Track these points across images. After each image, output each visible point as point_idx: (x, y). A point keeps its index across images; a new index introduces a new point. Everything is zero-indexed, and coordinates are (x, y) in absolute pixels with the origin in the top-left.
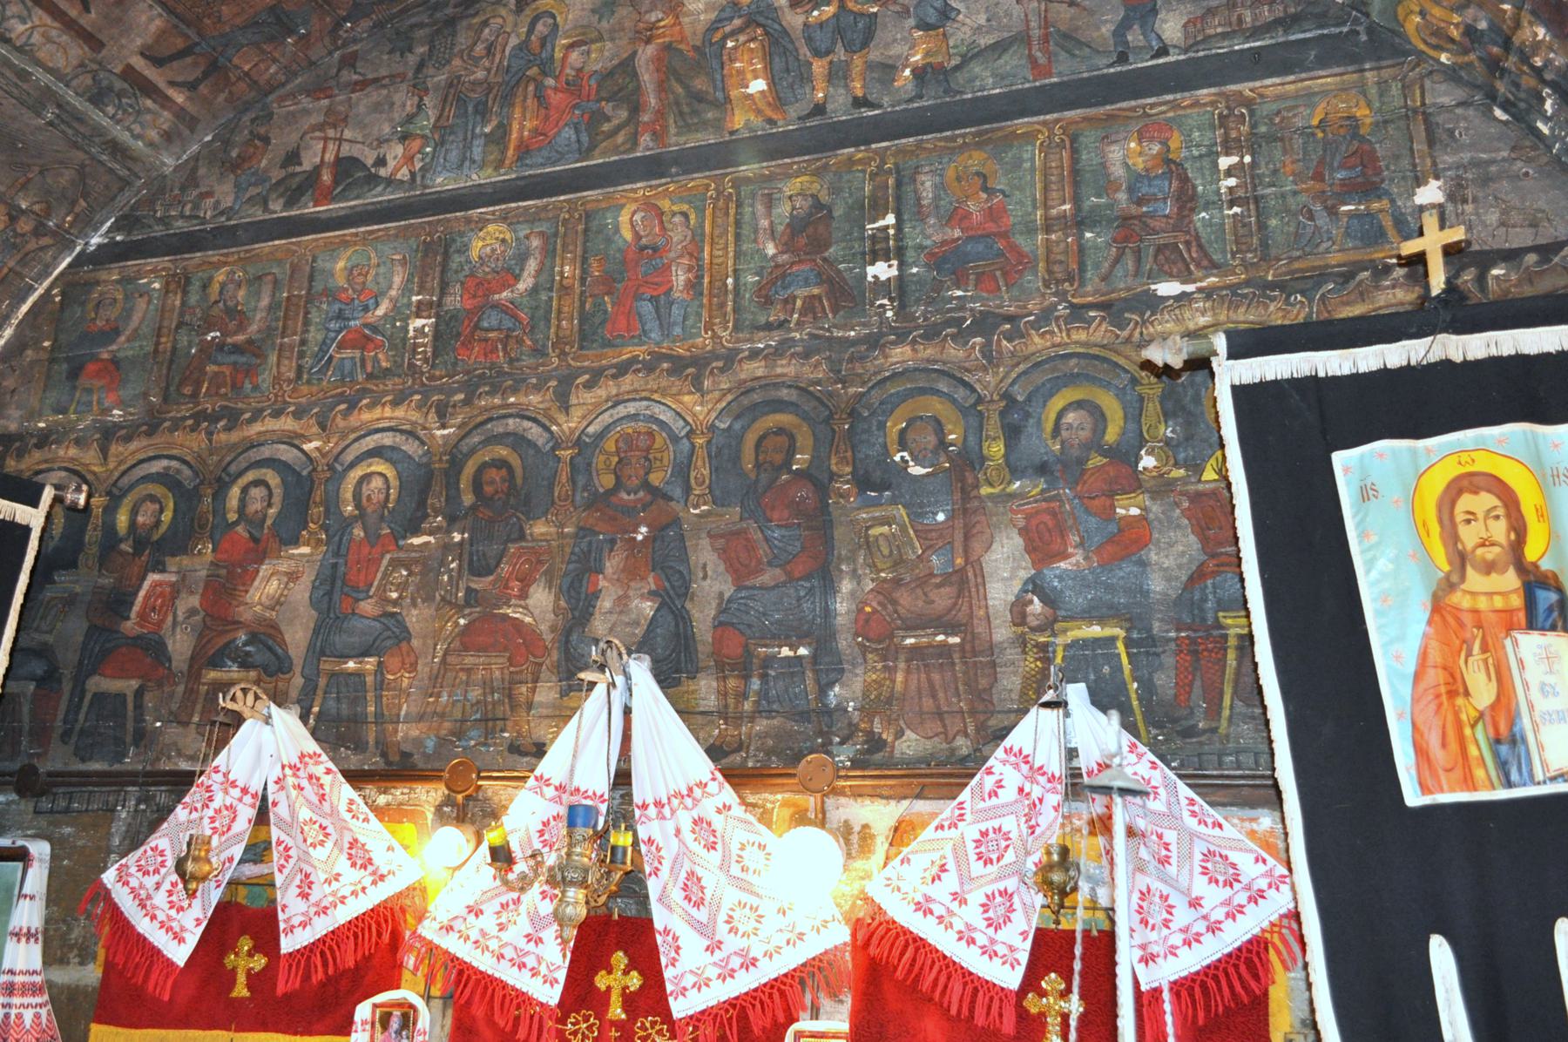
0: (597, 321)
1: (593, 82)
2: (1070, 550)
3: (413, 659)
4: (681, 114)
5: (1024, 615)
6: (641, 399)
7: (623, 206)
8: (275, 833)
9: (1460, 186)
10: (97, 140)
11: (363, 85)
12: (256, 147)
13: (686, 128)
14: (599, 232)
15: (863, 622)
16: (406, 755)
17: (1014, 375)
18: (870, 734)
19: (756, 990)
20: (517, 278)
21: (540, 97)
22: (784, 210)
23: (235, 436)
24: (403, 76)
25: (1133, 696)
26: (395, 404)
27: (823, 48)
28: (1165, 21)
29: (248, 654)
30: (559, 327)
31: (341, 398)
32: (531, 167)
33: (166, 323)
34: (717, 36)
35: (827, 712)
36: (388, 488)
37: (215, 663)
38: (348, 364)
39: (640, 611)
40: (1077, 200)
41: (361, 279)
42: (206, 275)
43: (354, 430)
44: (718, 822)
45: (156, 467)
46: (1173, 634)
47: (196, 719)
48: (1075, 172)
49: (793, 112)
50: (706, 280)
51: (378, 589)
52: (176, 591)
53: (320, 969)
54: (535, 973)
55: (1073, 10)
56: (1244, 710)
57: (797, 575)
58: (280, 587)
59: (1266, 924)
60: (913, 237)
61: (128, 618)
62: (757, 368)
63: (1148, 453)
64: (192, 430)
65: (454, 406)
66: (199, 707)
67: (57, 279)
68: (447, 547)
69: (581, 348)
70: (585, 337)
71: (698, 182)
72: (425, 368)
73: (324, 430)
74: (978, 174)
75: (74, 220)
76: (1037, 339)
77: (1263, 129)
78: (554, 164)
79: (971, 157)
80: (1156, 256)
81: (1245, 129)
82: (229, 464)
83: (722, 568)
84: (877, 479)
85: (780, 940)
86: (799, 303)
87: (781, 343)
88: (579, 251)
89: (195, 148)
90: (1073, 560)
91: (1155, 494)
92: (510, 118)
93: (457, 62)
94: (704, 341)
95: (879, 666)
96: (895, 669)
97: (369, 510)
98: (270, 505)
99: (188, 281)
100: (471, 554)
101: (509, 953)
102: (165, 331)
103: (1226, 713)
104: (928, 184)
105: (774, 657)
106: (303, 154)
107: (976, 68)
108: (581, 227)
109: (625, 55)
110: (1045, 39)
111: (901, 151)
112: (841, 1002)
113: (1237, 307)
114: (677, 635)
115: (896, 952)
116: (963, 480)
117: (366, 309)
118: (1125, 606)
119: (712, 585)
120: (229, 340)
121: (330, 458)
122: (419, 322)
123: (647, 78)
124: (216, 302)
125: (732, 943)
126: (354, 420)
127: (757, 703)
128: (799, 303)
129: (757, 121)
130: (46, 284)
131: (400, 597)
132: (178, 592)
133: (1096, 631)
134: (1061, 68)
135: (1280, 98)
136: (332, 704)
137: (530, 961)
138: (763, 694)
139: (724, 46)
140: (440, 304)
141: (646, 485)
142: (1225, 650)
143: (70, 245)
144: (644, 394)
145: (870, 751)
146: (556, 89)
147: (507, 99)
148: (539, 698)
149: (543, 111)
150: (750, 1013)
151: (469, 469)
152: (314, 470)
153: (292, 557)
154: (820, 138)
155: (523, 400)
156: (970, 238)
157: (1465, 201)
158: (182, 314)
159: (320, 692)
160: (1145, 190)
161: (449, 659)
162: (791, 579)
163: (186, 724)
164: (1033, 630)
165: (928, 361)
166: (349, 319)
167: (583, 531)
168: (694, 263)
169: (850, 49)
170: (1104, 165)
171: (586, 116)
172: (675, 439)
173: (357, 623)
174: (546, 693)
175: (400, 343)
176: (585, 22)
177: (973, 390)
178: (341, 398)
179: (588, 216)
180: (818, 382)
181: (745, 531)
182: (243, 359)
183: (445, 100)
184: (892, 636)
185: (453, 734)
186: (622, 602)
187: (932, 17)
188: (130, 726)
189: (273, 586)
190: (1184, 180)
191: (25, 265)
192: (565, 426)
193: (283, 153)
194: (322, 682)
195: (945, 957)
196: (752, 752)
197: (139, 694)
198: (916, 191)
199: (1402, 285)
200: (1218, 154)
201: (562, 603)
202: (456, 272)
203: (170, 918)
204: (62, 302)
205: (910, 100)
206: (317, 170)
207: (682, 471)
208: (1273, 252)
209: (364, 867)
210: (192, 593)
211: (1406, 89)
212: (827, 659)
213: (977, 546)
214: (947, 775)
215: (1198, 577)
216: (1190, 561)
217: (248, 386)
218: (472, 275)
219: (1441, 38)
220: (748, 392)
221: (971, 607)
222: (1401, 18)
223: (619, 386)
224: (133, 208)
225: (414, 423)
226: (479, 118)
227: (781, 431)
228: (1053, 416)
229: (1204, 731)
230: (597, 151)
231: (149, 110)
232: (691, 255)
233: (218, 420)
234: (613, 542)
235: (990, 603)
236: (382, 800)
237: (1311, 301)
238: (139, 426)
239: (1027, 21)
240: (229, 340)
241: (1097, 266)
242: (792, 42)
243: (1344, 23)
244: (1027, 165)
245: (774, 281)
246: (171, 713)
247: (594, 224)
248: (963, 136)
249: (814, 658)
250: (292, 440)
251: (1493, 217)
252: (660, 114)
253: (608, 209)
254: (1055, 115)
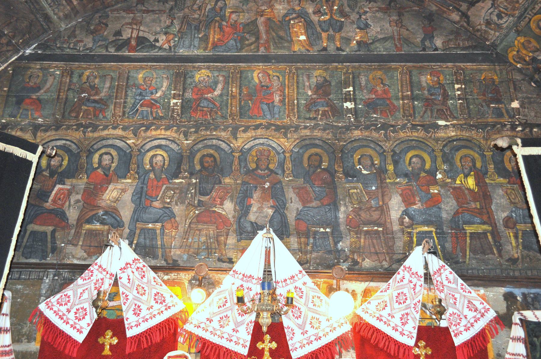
0: (247, 108)
1: (241, 26)
2: (417, 202)
3: (176, 225)
4: (275, 43)
5: (403, 222)
6: (265, 138)
7: (254, 71)
8: (121, 290)
9: (523, 103)
10: (41, 12)
11: (148, 11)
12: (102, 27)
13: (278, 48)
14: (245, 78)
15: (349, 222)
16: (175, 261)
17: (395, 144)
18: (353, 259)
19: (321, 348)
20: (214, 90)
21: (221, 28)
22: (314, 80)
23: (96, 135)
24: (164, 12)
25: (439, 250)
26: (166, 129)
27: (325, 29)
28: (436, 40)
29: (104, 219)
30: (231, 109)
31: (143, 125)
32: (218, 52)
33: (62, 88)
34: (287, 19)
35: (338, 251)
36: (164, 160)
37: (89, 221)
38: (145, 113)
39: (267, 212)
40: (412, 91)
41: (150, 82)
42: (81, 72)
43: (148, 138)
44: (304, 289)
45: (60, 143)
46: (450, 231)
47: (81, 243)
48: (411, 82)
49: (316, 48)
50: (287, 100)
51: (161, 197)
52: (69, 193)
53: (145, 343)
54: (237, 343)
55: (408, 32)
56: (473, 256)
57: (325, 204)
58: (119, 194)
59: (486, 324)
60: (359, 95)
61: (47, 202)
62: (307, 132)
63: (440, 173)
64: (76, 130)
65: (191, 133)
66: (82, 239)
67: (10, 64)
68: (190, 184)
69: (241, 118)
70: (241, 115)
71: (282, 67)
72: (178, 118)
73: (136, 135)
74: (380, 78)
76: (402, 134)
77: (467, 78)
78: (227, 52)
79: (377, 73)
80: (437, 112)
81: (462, 77)
82: (94, 145)
83: (298, 199)
84: (351, 174)
85: (328, 330)
86: (320, 112)
87: (315, 124)
88: (238, 84)
89: (74, 23)
90: (418, 205)
91: (442, 187)
92: (209, 33)
93: (186, 10)
94: (287, 121)
95: (355, 236)
96: (361, 238)
97: (156, 168)
98: (112, 162)
99: (72, 73)
100: (200, 187)
101: (226, 336)
102: (62, 91)
103: (468, 257)
104: (363, 79)
105: (317, 231)
106: (123, 32)
107: (378, 45)
108: (238, 76)
109: (253, 19)
110: (399, 39)
111: (354, 67)
112: (349, 351)
113: (463, 131)
114: (282, 221)
115: (370, 334)
116: (380, 177)
117: (152, 93)
118: (435, 221)
119: (294, 206)
120: (92, 98)
121: (139, 147)
122: (175, 101)
123: (262, 28)
124: (85, 83)
125: (311, 332)
126: (149, 134)
127: (312, 247)
128: (320, 112)
129: (303, 49)
130: (6, 65)
131: (171, 201)
132: (71, 193)
133: (426, 229)
134: (405, 49)
135: (472, 69)
136: (142, 240)
137: (235, 339)
138: (314, 244)
139: (290, 22)
140: (183, 95)
141: (268, 168)
142: (466, 237)
143: (17, 51)
144: (266, 137)
145: (354, 265)
146: (227, 26)
147: (208, 26)
148: (229, 242)
149: (222, 33)
150: (319, 356)
151: (198, 156)
152: (132, 151)
153: (123, 183)
154: (326, 58)
155: (219, 134)
156: (378, 99)
157: (525, 108)
158: (70, 85)
159: (137, 235)
160: (433, 91)
161: (192, 226)
162: (323, 205)
163: (76, 245)
164: (406, 227)
165: (366, 136)
166: (145, 96)
167: (244, 183)
168: (282, 93)
169: (334, 30)
170: (420, 82)
171: (239, 38)
172: (278, 153)
173: (151, 209)
174: (232, 240)
175: (167, 107)
176: (237, 5)
177: (382, 148)
178: (143, 125)
179: (241, 72)
180: (329, 139)
181: (306, 187)
182: (98, 106)
183: (182, 23)
184: (359, 227)
185: (195, 254)
186: (260, 209)
187: (362, 26)
188: (49, 245)
189: (115, 194)
190: (445, 90)
192: (236, 145)
193: (114, 31)
194: (138, 232)
195: (387, 335)
196: (311, 264)
197: (53, 232)
198: (359, 80)
199: (509, 130)
200: (454, 84)
201: (237, 208)
202: (189, 85)
203: (75, 323)
204: (13, 73)
205: (356, 51)
206: (129, 39)
207: (282, 165)
208: (472, 116)
209: (161, 303)
210: (77, 193)
211: (507, 73)
212: (337, 233)
213: (386, 198)
214: (386, 275)
215: (457, 213)
216: (454, 208)
217: (101, 116)
218: (196, 86)
219: (521, 59)
220: (304, 140)
221: (385, 218)
222: (508, 52)
223: (256, 133)
224: (45, 41)
225: (174, 138)
226: (196, 31)
227: (317, 154)
228: (408, 159)
229: (462, 262)
230: (244, 50)
231: (63, 5)
232: (281, 91)
233: (87, 128)
234: (256, 187)
235: (392, 218)
236: (166, 278)
237: (484, 132)
238: (51, 126)
239: (394, 33)
240: (92, 98)
241: (419, 113)
242: (314, 25)
243: (489, 50)
244: (396, 78)
245: (311, 105)
246: (68, 241)
247: (244, 75)
248: (374, 65)
249: (332, 233)
250: (122, 138)
251: (533, 114)
252: (267, 41)
253: (249, 71)
254: (404, 64)
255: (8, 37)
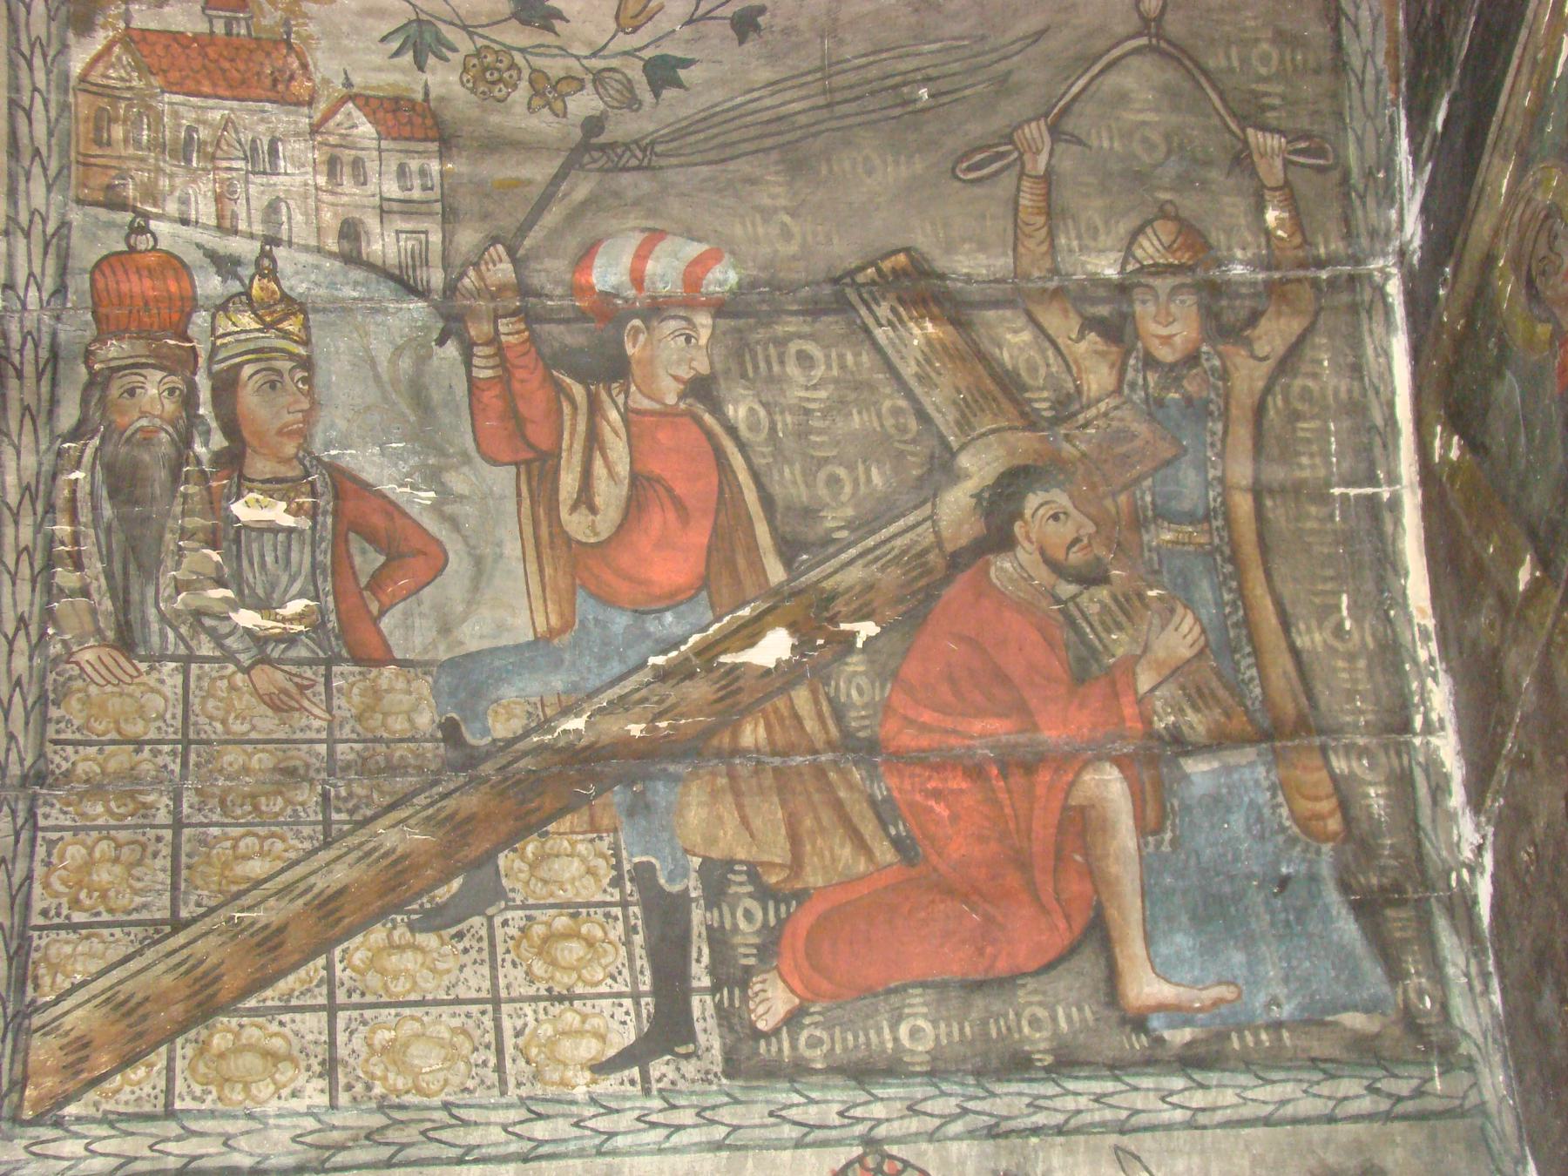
75: (1292, 201)
143: (1351, 299)
191: (1288, 454)
255: (1163, 284)
